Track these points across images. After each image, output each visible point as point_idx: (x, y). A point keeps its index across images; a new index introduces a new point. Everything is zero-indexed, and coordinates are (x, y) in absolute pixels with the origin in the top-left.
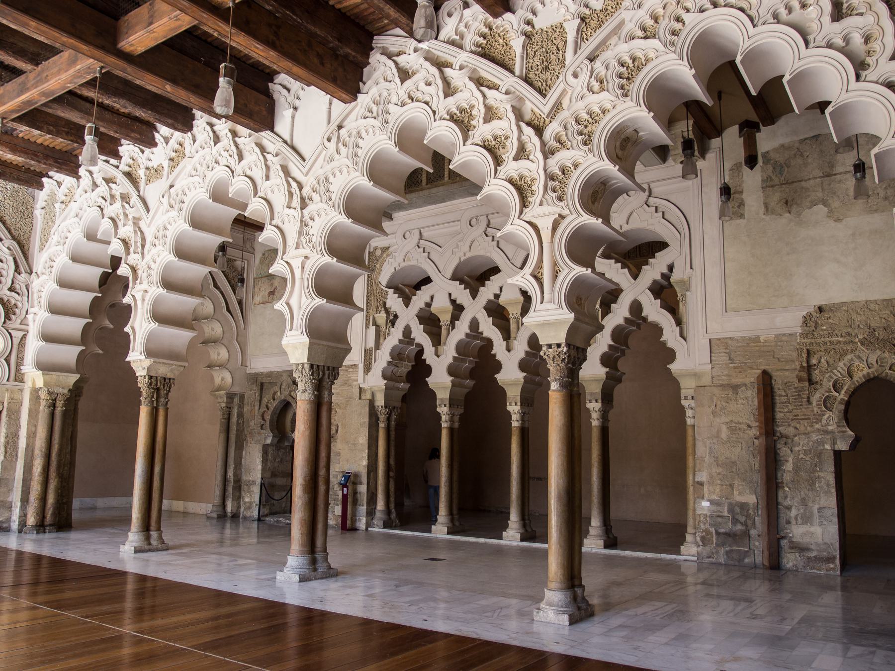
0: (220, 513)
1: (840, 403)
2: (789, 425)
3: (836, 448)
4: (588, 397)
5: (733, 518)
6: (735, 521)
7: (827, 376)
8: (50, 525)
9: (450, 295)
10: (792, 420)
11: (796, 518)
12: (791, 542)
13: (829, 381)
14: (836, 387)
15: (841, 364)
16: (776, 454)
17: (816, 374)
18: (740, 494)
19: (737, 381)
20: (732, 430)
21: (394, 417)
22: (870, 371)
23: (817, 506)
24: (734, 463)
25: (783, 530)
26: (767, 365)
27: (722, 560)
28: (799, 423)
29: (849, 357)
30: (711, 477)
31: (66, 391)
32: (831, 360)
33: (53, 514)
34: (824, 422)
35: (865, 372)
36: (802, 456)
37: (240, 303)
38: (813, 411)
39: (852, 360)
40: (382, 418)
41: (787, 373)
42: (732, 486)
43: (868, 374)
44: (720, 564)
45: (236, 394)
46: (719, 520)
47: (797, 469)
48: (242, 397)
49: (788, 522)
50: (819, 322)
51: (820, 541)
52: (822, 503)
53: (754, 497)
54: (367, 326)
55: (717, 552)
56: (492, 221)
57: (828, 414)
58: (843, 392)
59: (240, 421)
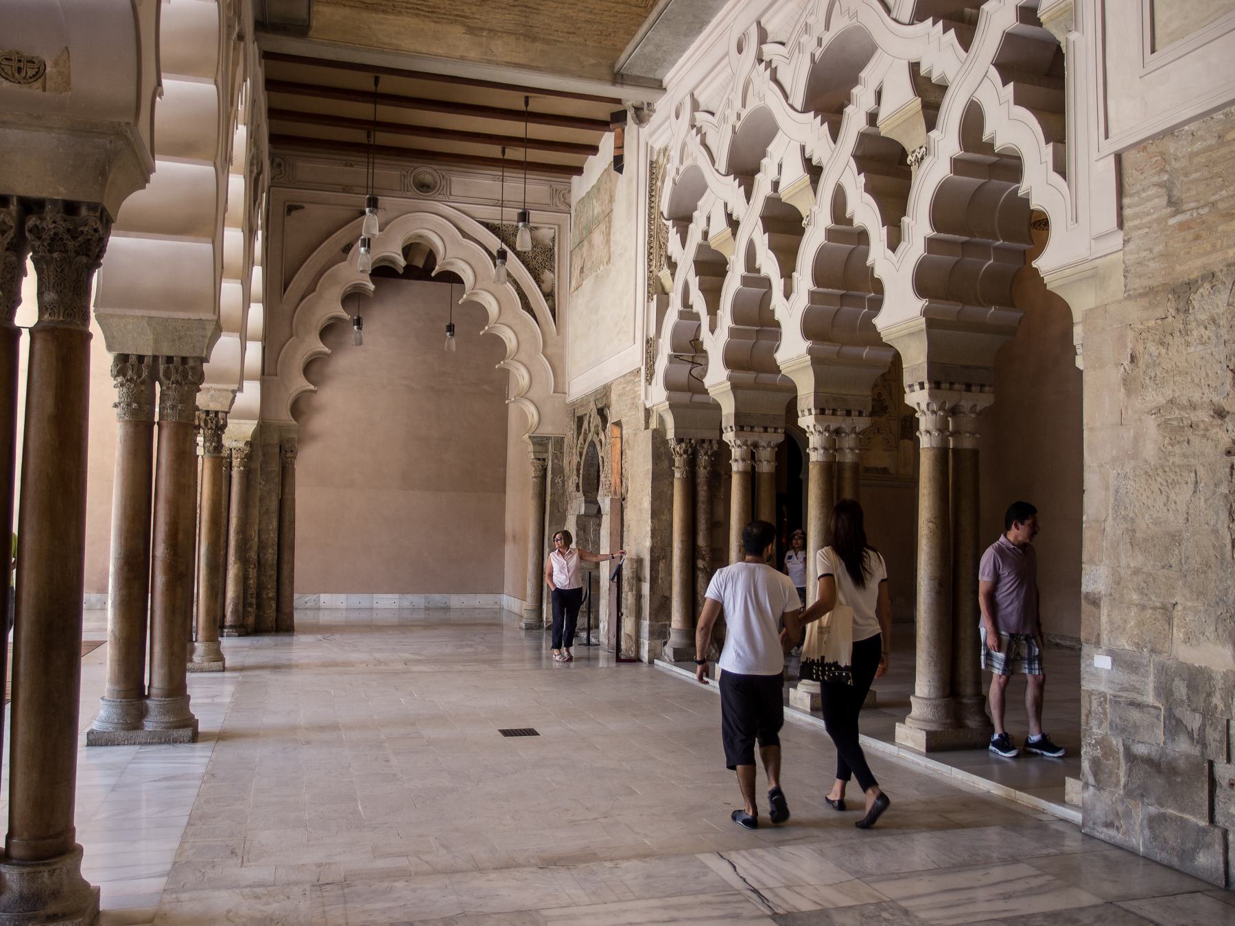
0: (529, 621)
4: (907, 379)
5: (1170, 715)
6: (1174, 726)
8: (231, 627)
9: (726, 205)
18: (1187, 640)
19: (1190, 268)
20: (1177, 431)
21: (703, 459)
24: (1175, 539)
27: (1138, 840)
30: (1118, 582)
31: (241, 445)
33: (235, 611)
37: (549, 296)
40: (678, 461)
42: (1167, 611)
44: (1133, 852)
45: (548, 438)
46: (1135, 715)
48: (560, 442)
54: (650, 298)
55: (1128, 814)
56: (769, 28)
59: (558, 480)
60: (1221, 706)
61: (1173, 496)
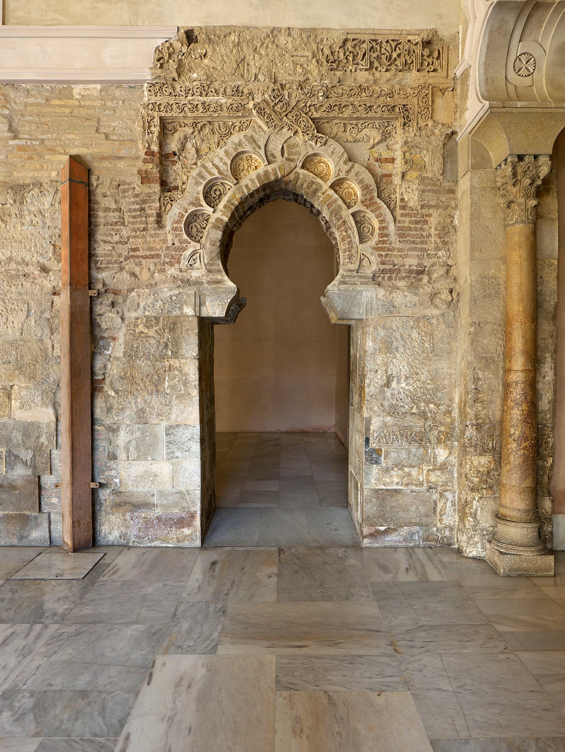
1: (215, 227)
2: (121, 269)
3: (204, 314)
7: (194, 173)
10: (127, 258)
11: (127, 449)
12: (116, 493)
13: (197, 183)
14: (211, 195)
15: (221, 152)
16: (93, 324)
17: (177, 173)
19: (24, 175)
22: (270, 168)
23: (164, 424)
25: (103, 472)
26: (85, 145)
28: (140, 264)
29: (236, 137)
32: (204, 148)
34: (184, 263)
35: (261, 170)
36: (141, 328)
38: (165, 241)
39: (240, 144)
41: (121, 165)
43: (266, 172)
47: (131, 354)
49: (113, 457)
50: (186, 61)
51: (168, 488)
52: (173, 417)
53: (51, 411)
57: (193, 246)
58: (221, 206)
60: (46, 443)
61: (11, 318)
